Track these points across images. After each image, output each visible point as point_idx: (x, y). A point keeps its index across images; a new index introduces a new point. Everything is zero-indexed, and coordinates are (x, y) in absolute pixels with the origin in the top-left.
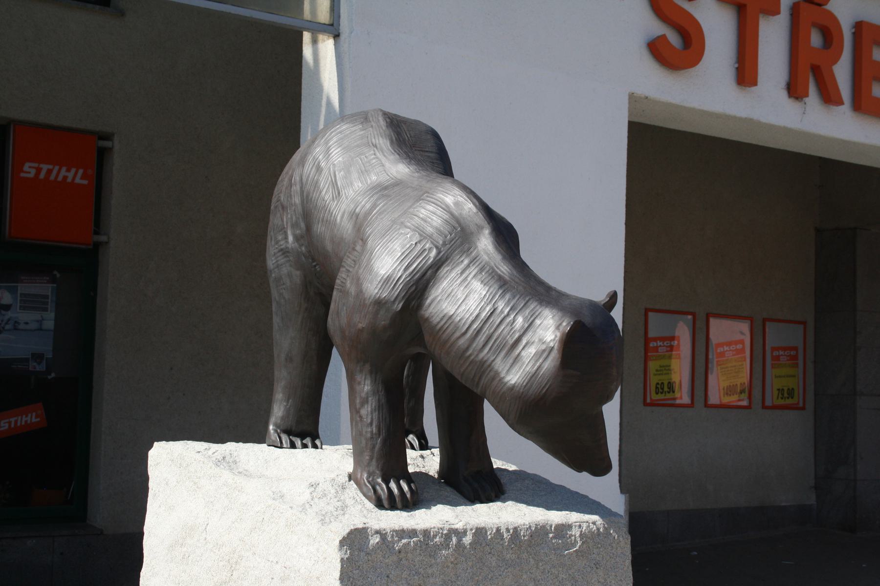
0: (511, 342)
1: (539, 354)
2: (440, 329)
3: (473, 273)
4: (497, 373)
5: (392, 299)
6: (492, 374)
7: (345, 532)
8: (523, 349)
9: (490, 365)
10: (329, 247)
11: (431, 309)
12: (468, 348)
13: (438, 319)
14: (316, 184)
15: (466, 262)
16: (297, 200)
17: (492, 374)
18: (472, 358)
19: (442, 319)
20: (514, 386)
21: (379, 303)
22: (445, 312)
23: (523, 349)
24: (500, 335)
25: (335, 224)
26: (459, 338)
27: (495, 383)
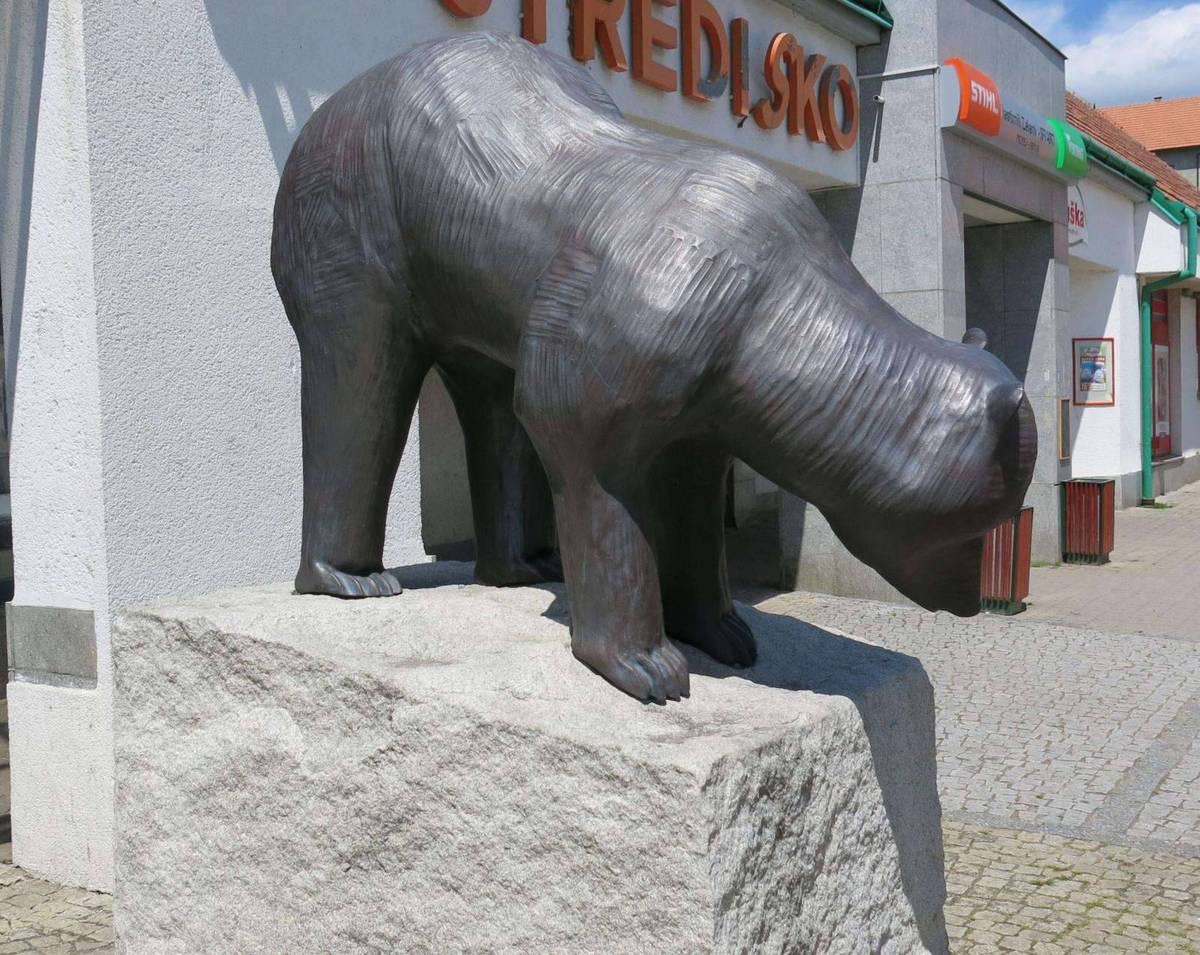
0: (903, 421)
1: (954, 438)
2: (770, 406)
3: (816, 307)
4: (882, 473)
5: (691, 353)
6: (871, 474)
7: (945, 619)
8: (924, 429)
9: (869, 460)
10: (482, 264)
11: (752, 369)
12: (826, 435)
13: (767, 387)
14: (430, 156)
15: (798, 289)
16: (381, 182)
17: (871, 474)
18: (836, 449)
19: (773, 387)
20: (915, 493)
21: (663, 363)
22: (781, 373)
23: (924, 429)
24: (882, 409)
25: (497, 223)
26: (809, 418)
27: (876, 490)
